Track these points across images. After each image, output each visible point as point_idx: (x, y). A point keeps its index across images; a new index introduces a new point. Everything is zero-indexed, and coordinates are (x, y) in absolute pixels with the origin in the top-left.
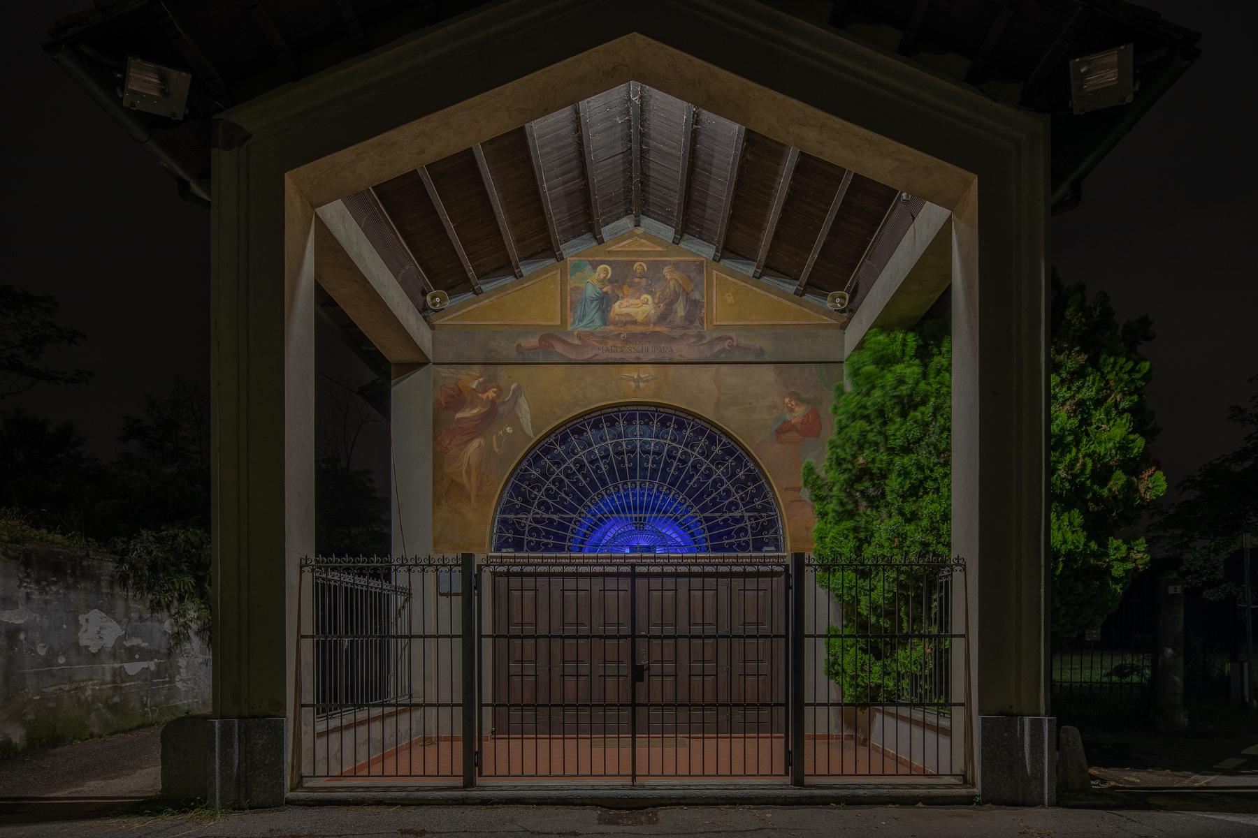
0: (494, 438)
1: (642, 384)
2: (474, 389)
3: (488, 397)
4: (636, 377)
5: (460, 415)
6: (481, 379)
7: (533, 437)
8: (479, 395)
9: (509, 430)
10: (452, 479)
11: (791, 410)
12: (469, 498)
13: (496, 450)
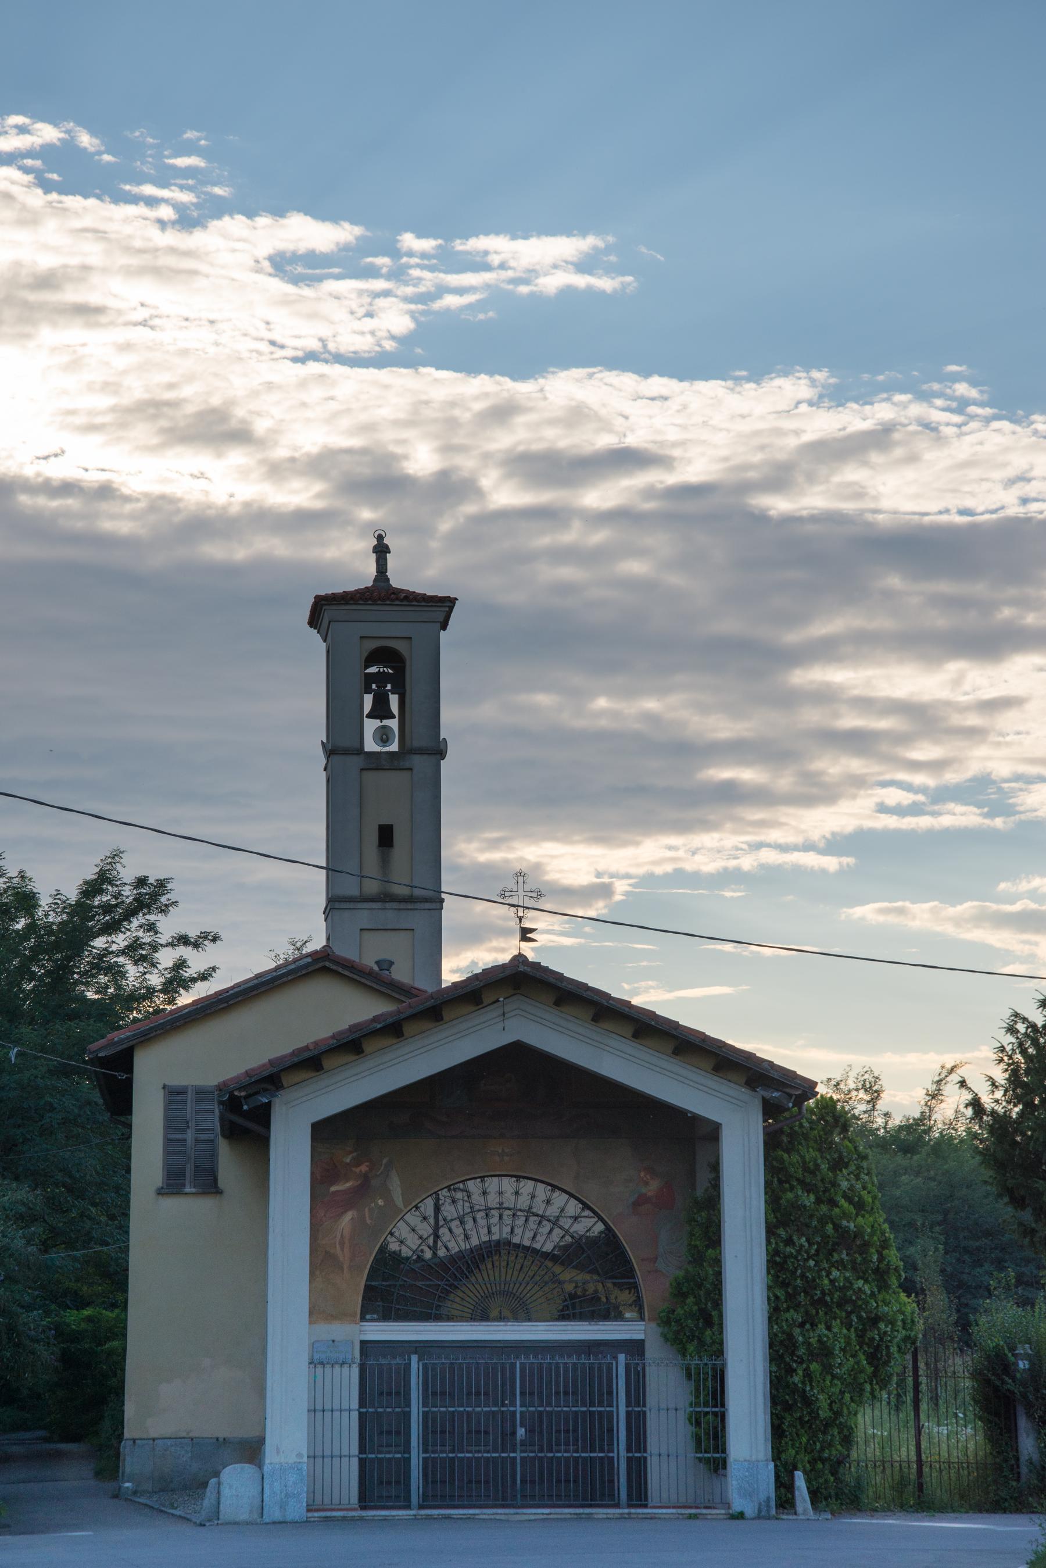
0: (367, 1209)
1: (506, 1158)
2: (348, 1164)
3: (361, 1171)
4: (500, 1151)
5: (333, 1189)
6: (355, 1154)
7: (403, 1208)
8: (354, 1169)
9: (380, 1202)
10: (326, 1252)
11: (647, 1184)
12: (342, 1269)
13: (369, 1222)
